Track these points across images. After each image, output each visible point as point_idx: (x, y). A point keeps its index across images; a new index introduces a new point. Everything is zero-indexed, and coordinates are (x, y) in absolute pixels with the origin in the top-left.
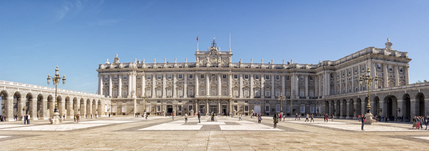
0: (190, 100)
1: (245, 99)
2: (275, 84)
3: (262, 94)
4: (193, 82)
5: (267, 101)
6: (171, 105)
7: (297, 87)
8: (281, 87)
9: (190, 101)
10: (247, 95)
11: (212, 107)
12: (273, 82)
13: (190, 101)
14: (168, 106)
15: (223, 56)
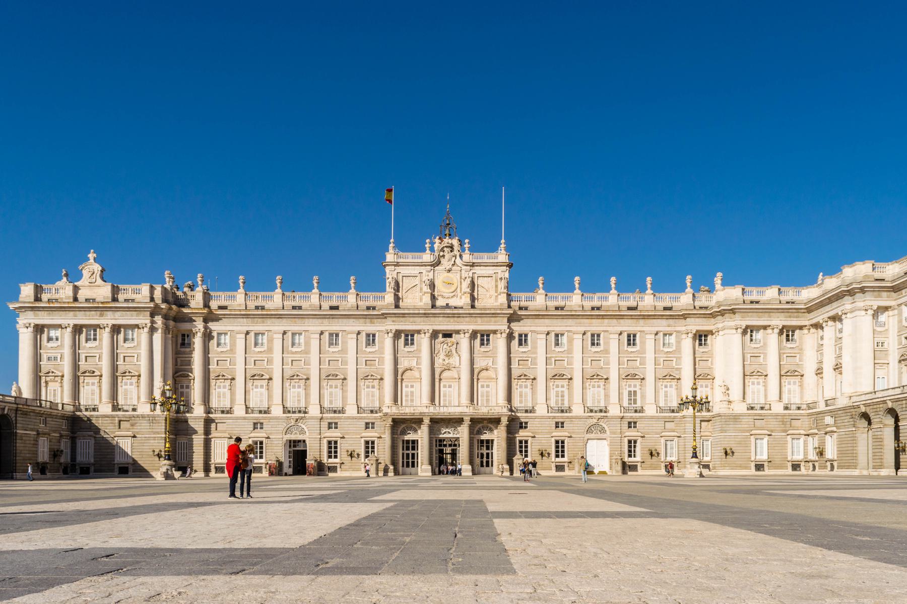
0: (367, 421)
1: (554, 418)
4: (377, 360)
6: (304, 441)
8: (680, 373)
9: (367, 424)
10: (563, 404)
12: (650, 355)
13: (367, 424)
14: (290, 441)
15: (479, 271)
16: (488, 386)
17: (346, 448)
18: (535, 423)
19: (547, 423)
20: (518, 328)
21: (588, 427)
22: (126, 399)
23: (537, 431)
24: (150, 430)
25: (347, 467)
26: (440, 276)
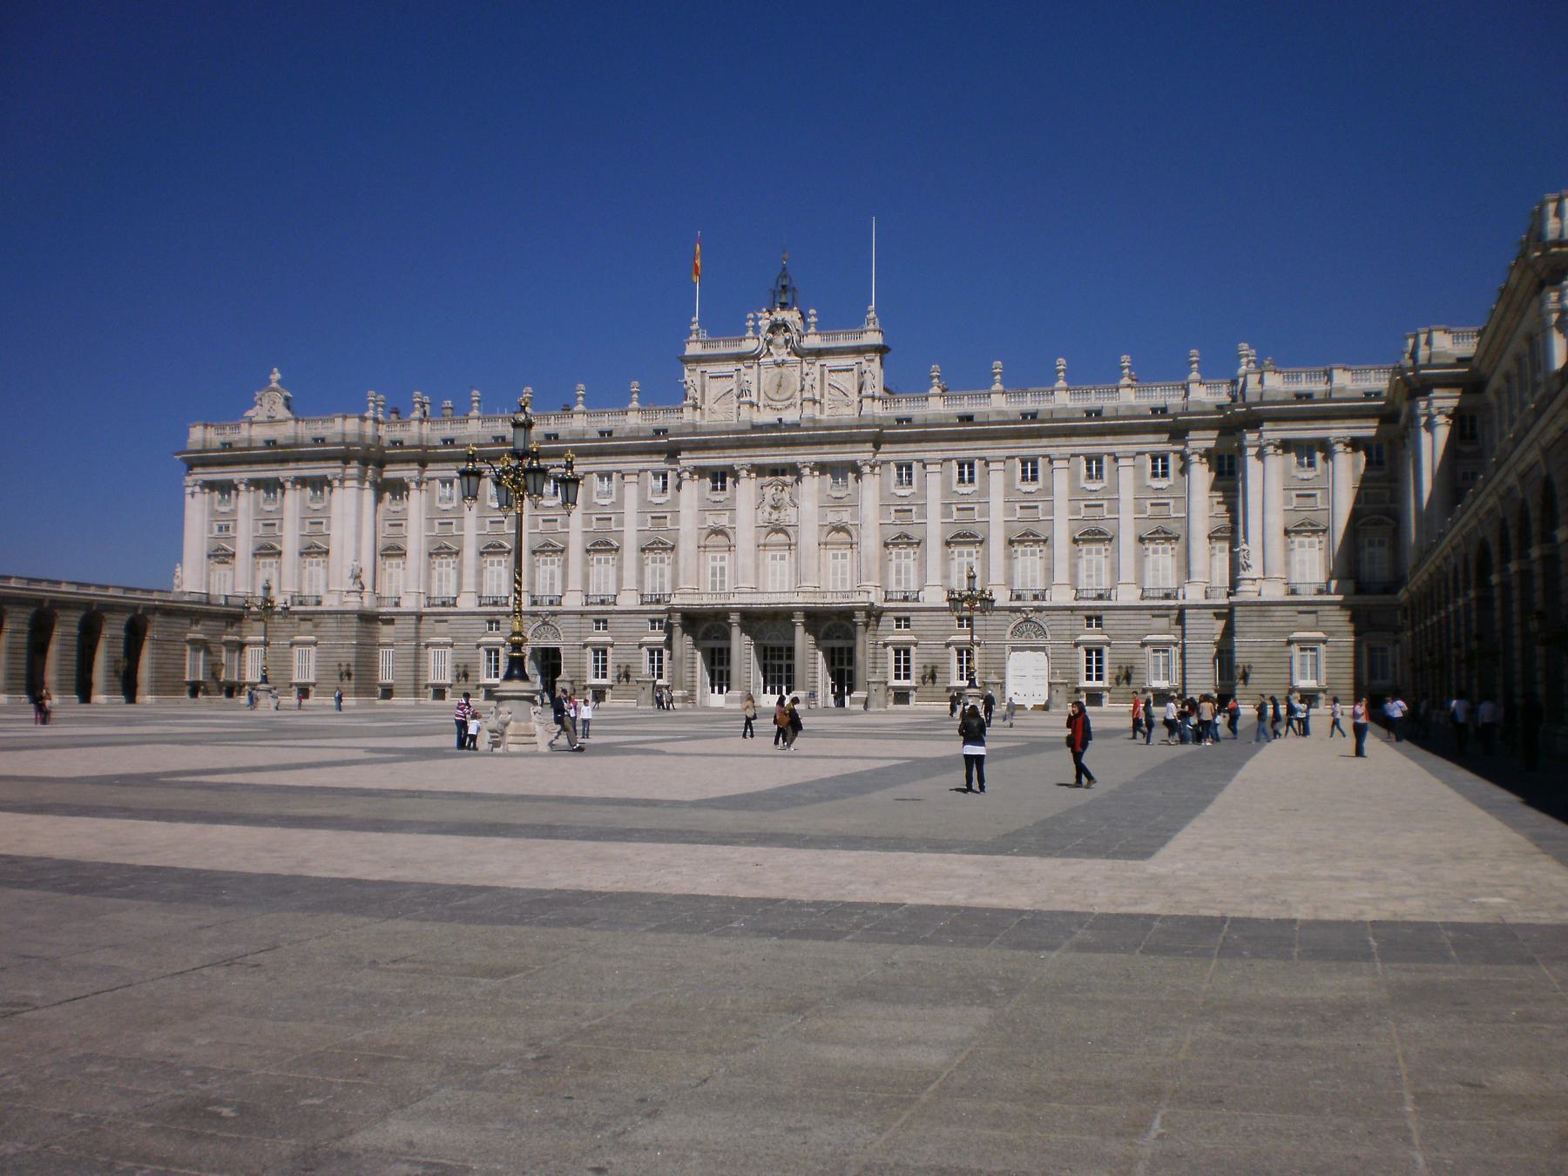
0: (651, 616)
2: (1139, 509)
3: (1061, 575)
5: (1094, 619)
7: (1276, 522)
11: (780, 657)
16: (844, 556)
17: (619, 661)
18: (921, 618)
19: (941, 618)
20: (889, 453)
21: (1012, 626)
22: (311, 586)
23: (924, 633)
24: (338, 634)
25: (621, 692)
26: (768, 376)
